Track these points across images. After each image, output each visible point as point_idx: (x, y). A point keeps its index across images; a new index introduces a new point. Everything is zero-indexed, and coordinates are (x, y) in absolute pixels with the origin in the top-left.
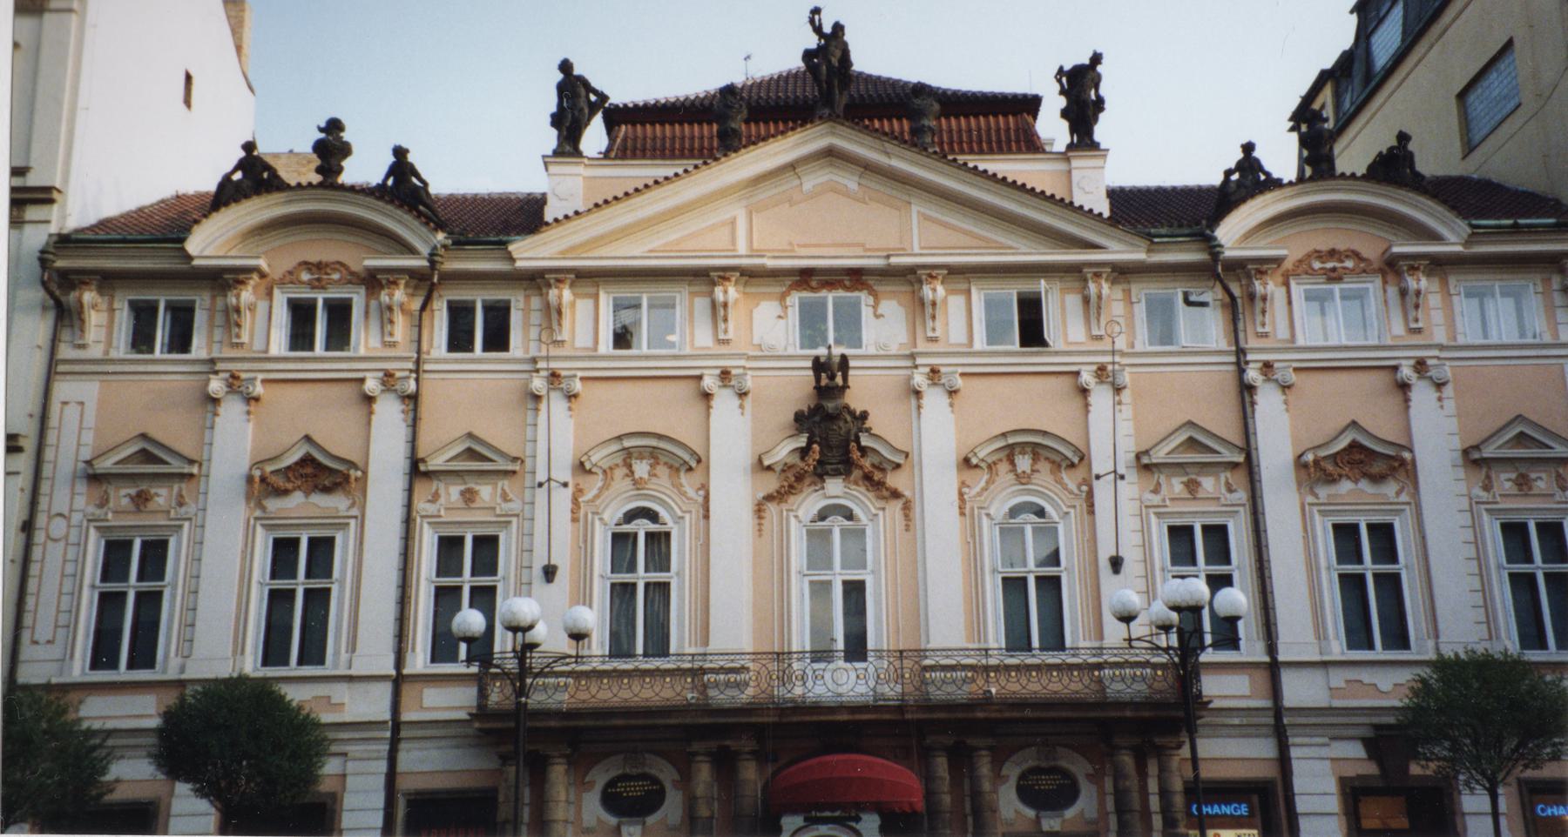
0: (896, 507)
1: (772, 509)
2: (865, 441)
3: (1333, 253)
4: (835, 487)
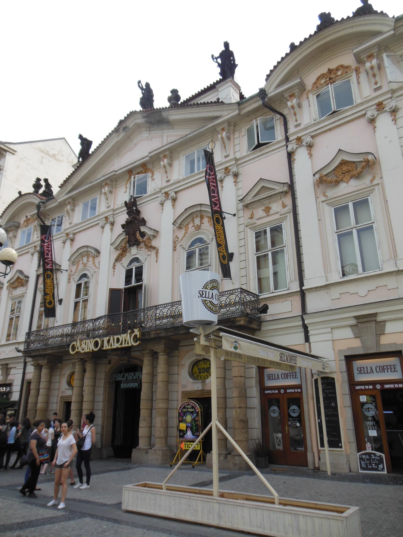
0: (153, 253)
1: (118, 265)
2: (143, 229)
3: (330, 71)
4: (134, 251)
